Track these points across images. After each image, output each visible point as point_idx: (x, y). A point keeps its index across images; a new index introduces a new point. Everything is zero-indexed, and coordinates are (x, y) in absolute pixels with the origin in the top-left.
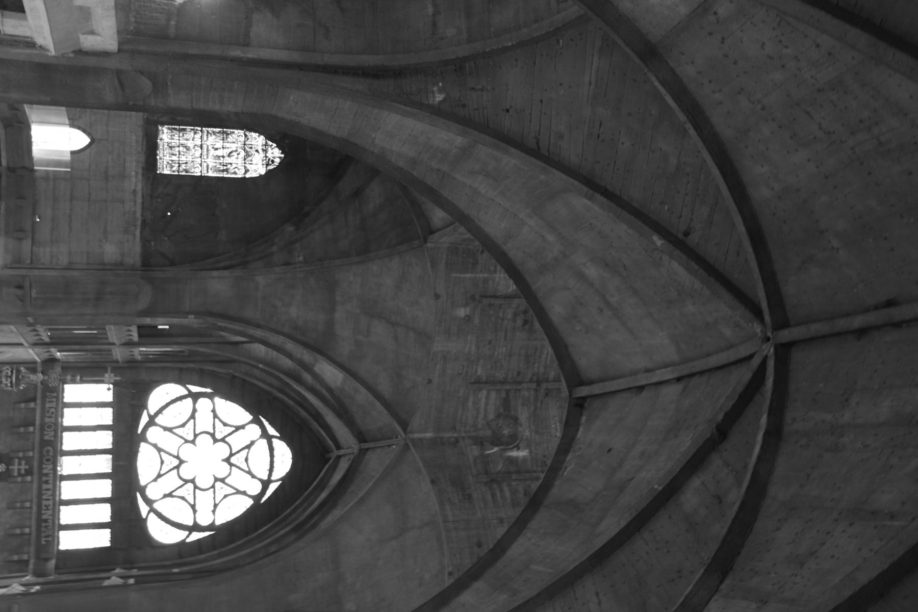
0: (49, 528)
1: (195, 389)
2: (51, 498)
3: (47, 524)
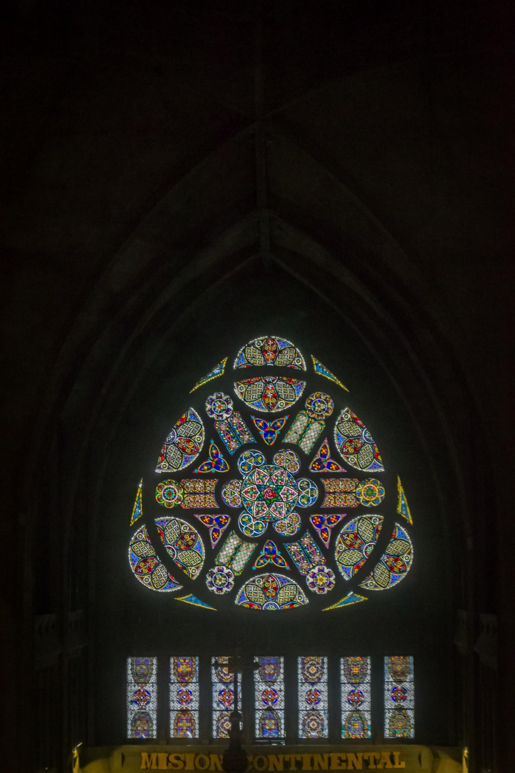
0: (378, 757)
1: (138, 510)
2: (326, 756)
3: (372, 761)
